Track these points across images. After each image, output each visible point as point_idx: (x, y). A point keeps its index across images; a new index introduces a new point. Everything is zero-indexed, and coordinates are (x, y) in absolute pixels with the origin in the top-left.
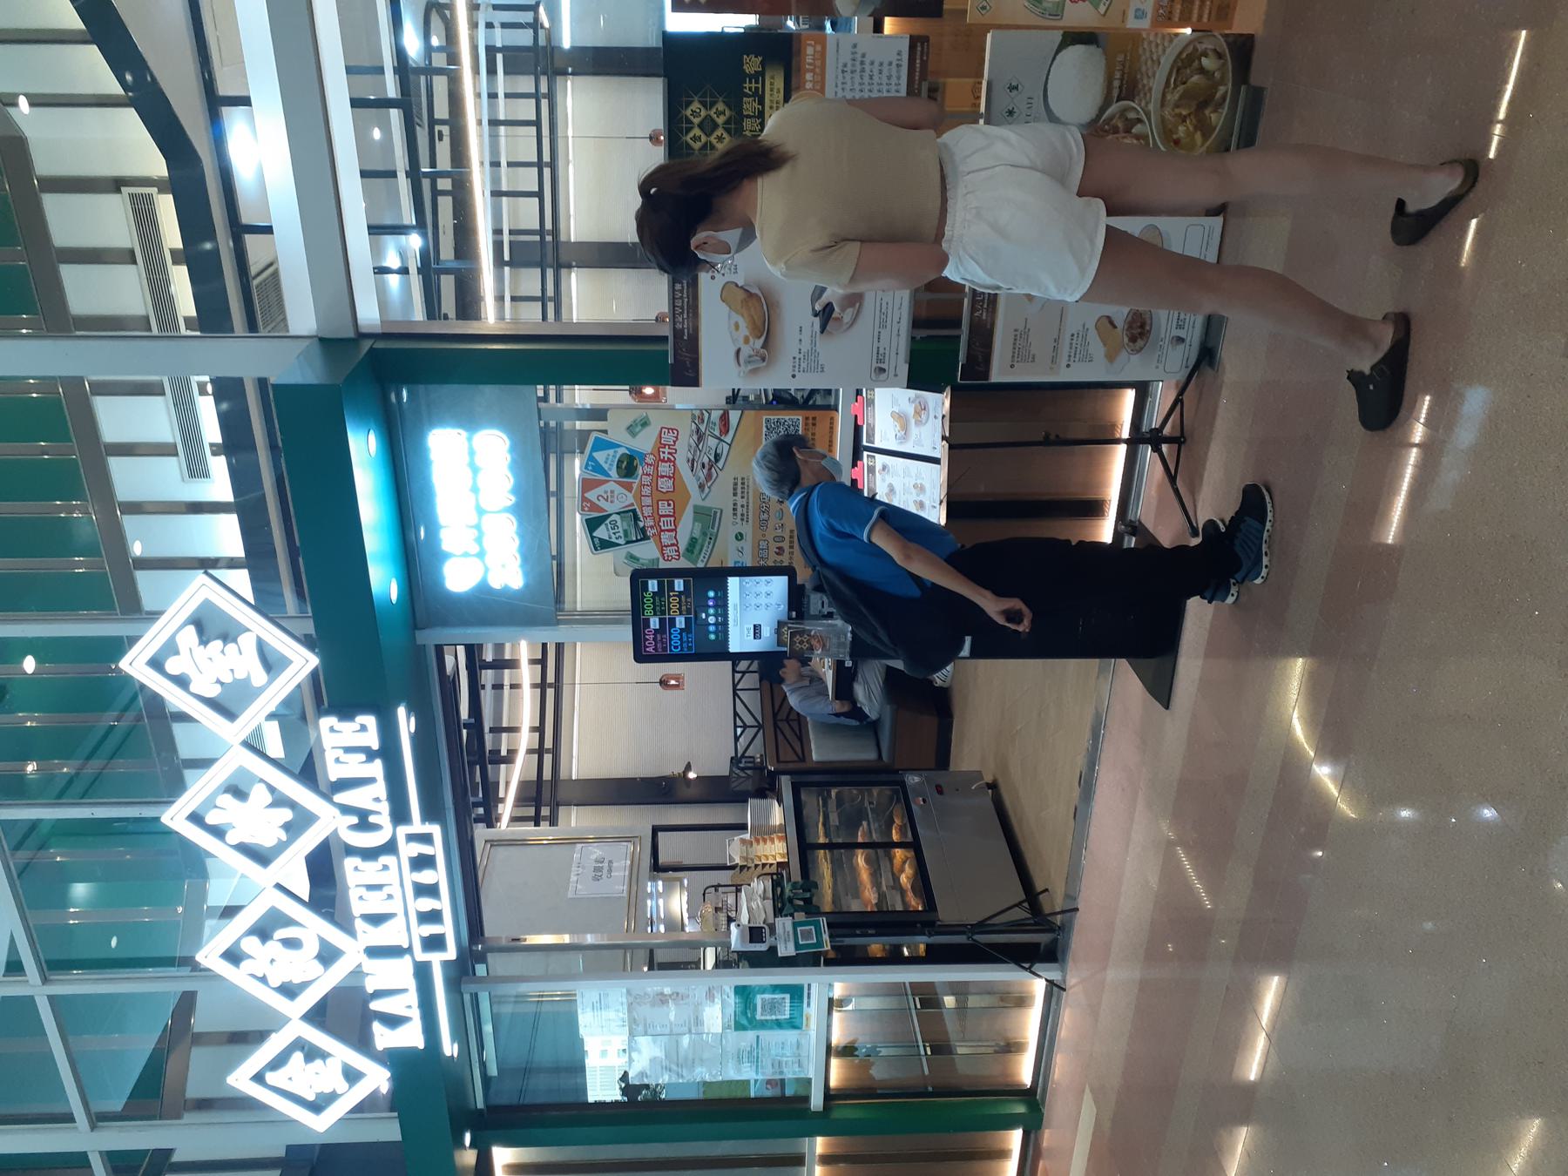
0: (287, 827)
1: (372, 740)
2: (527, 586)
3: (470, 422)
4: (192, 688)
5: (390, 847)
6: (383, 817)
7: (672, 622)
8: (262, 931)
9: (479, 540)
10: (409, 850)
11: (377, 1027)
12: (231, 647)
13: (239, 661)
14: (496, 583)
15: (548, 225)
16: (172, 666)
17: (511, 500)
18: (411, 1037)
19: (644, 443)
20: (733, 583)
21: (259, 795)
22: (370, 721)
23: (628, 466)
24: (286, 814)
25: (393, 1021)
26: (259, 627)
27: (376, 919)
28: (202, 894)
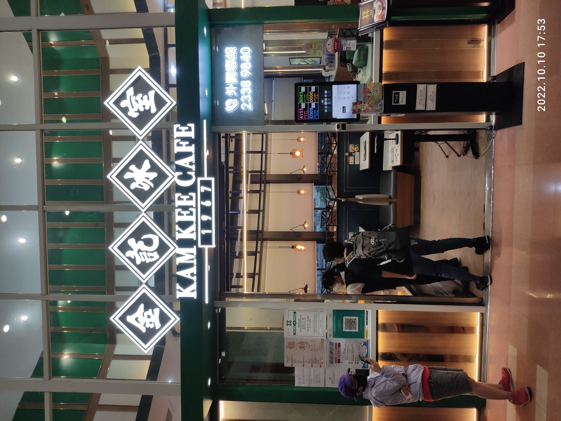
0: (153, 181)
1: (192, 134)
2: (254, 110)
3: (239, 45)
4: (129, 114)
6: (193, 174)
7: (310, 105)
8: (137, 235)
10: (202, 189)
11: (178, 286)
12: (146, 97)
13: (147, 102)
15: (263, 169)
16: (123, 104)
18: (190, 292)
21: (146, 165)
22: (192, 126)
24: (154, 175)
25: (185, 283)
27: (184, 225)
28: (113, 349)
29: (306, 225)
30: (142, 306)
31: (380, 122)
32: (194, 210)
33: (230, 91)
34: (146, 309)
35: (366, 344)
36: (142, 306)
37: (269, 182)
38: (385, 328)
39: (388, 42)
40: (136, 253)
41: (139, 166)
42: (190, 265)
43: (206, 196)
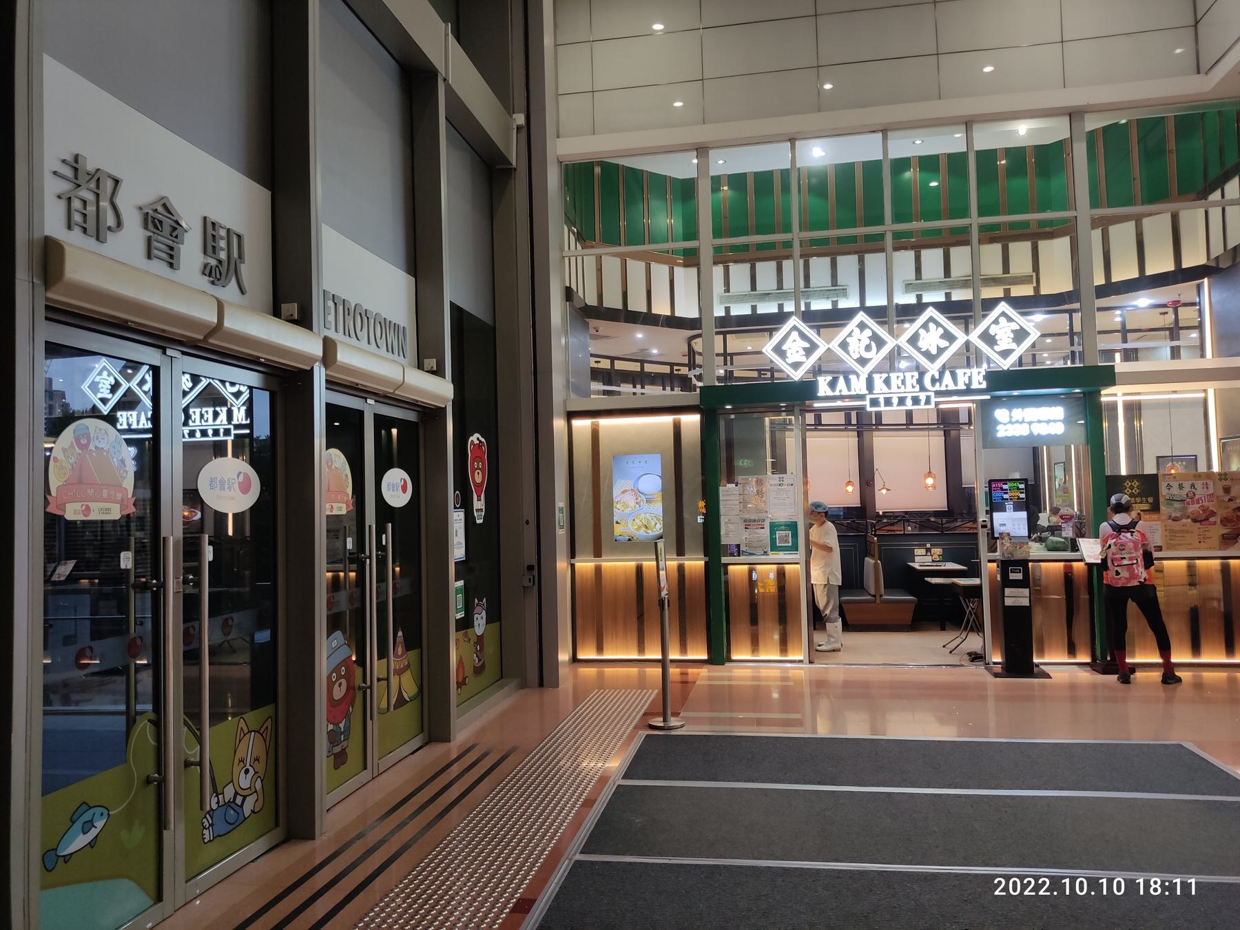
1: (975, 386)
3: (1066, 421)
5: (923, 389)
6: (937, 387)
8: (875, 338)
9: (1017, 422)
10: (923, 396)
11: (829, 378)
13: (1005, 342)
14: (999, 427)
17: (1036, 433)
18: (823, 389)
21: (944, 344)
22: (984, 385)
24: (934, 352)
25: (832, 384)
26: (1020, 350)
27: (887, 382)
28: (679, 265)
29: (884, 491)
30: (808, 345)
31: (990, 561)
32: (903, 389)
33: (1018, 413)
34: (805, 349)
35: (765, 553)
36: (808, 345)
37: (860, 435)
39: (1071, 567)
41: (942, 337)
42: (849, 389)
43: (916, 401)
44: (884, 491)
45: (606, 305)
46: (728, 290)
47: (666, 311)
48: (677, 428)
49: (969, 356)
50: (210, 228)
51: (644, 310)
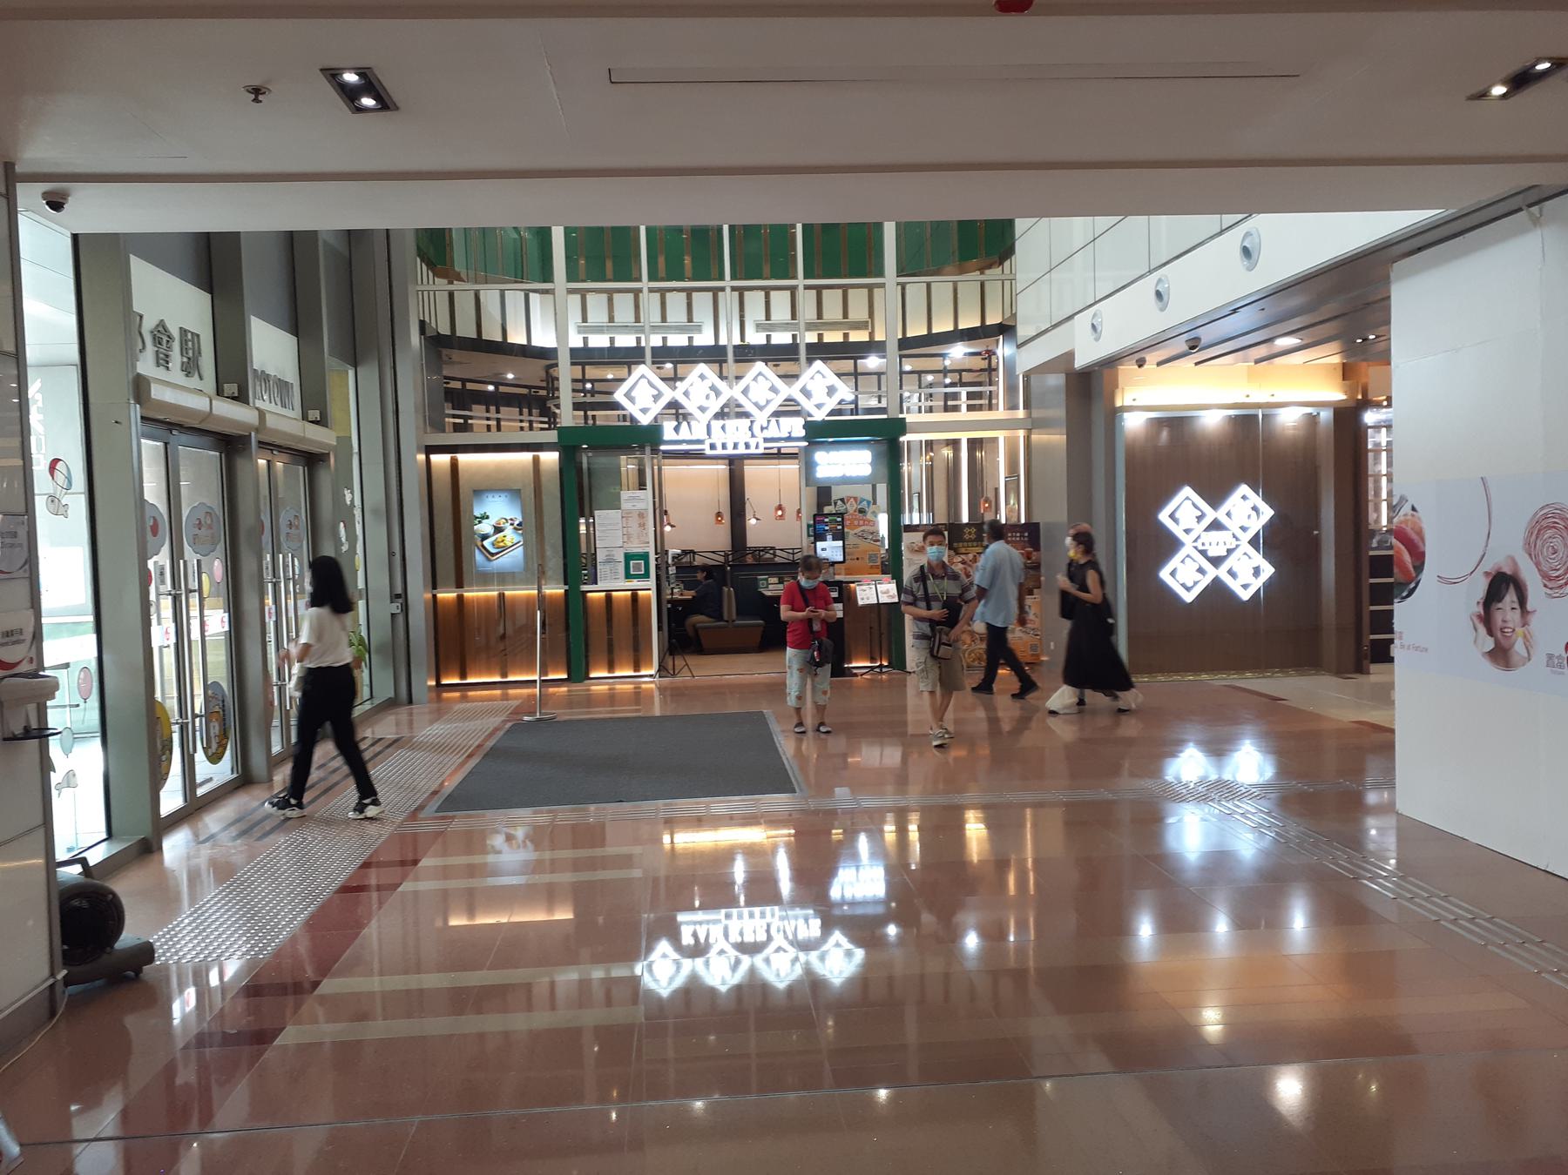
6: (767, 434)
10: (753, 443)
13: (819, 394)
14: (818, 469)
18: (668, 431)
19: (869, 516)
20: (840, 543)
23: (862, 511)
25: (677, 429)
38: (635, 597)
40: (699, 385)
43: (747, 446)
44: (753, 521)
45: (459, 334)
46: (585, 319)
47: (522, 340)
48: (536, 461)
49: (790, 409)
50: (183, 332)
51: (499, 339)
